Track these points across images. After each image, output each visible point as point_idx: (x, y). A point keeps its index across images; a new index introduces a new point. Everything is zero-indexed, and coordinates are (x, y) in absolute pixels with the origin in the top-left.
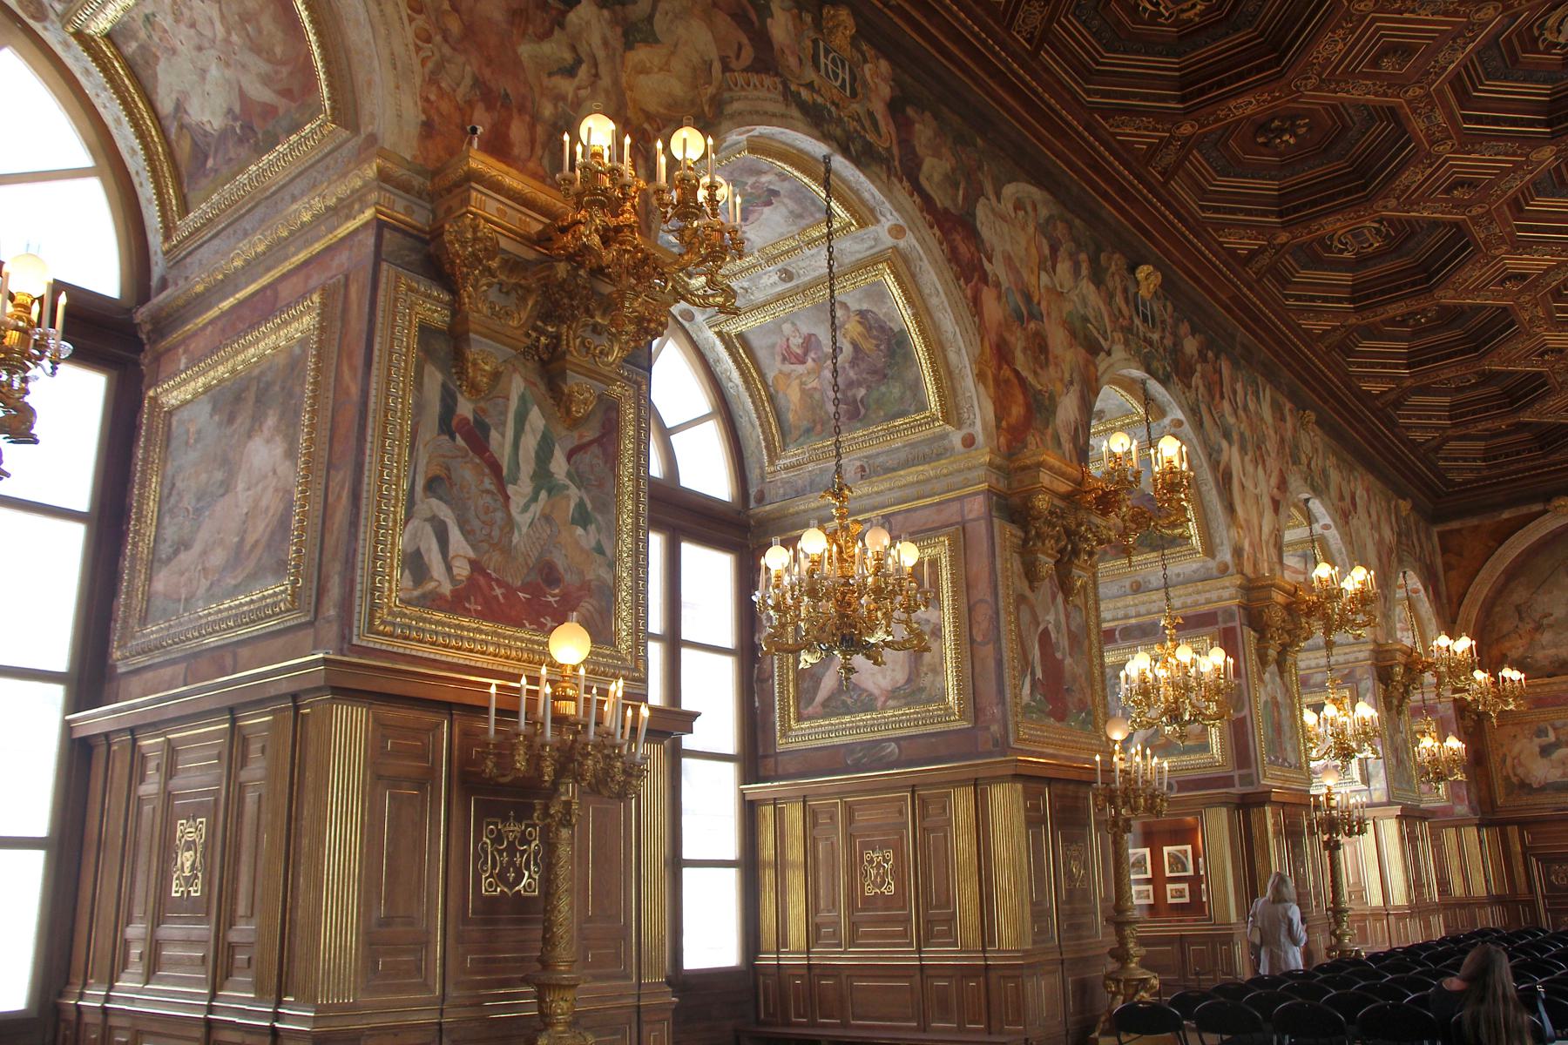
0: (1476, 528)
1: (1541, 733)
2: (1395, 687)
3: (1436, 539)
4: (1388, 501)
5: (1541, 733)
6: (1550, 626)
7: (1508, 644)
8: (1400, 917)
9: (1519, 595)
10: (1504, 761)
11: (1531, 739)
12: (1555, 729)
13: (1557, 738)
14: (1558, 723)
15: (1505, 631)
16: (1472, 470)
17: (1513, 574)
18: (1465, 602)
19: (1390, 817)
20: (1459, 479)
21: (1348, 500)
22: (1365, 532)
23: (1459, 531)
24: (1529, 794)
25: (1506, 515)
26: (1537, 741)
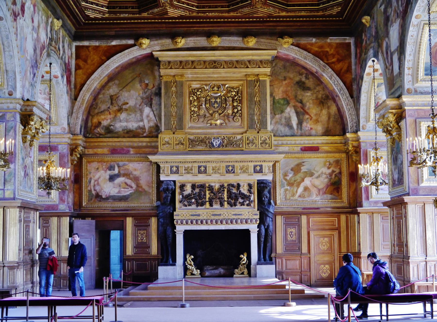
0: (96, 47)
1: (111, 168)
2: (30, 129)
3: (74, 50)
4: (48, 18)
5: (111, 168)
6: (126, 110)
7: (103, 117)
8: (11, 268)
9: (113, 90)
10: (90, 182)
11: (106, 171)
12: (119, 167)
13: (119, 172)
14: (121, 163)
15: (102, 109)
16: (100, 12)
17: (111, 78)
18: (84, 89)
19: (14, 207)
20: (92, 16)
21: (19, 6)
22: (28, 31)
23: (87, 47)
24: (100, 201)
25: (114, 43)
26: (109, 172)
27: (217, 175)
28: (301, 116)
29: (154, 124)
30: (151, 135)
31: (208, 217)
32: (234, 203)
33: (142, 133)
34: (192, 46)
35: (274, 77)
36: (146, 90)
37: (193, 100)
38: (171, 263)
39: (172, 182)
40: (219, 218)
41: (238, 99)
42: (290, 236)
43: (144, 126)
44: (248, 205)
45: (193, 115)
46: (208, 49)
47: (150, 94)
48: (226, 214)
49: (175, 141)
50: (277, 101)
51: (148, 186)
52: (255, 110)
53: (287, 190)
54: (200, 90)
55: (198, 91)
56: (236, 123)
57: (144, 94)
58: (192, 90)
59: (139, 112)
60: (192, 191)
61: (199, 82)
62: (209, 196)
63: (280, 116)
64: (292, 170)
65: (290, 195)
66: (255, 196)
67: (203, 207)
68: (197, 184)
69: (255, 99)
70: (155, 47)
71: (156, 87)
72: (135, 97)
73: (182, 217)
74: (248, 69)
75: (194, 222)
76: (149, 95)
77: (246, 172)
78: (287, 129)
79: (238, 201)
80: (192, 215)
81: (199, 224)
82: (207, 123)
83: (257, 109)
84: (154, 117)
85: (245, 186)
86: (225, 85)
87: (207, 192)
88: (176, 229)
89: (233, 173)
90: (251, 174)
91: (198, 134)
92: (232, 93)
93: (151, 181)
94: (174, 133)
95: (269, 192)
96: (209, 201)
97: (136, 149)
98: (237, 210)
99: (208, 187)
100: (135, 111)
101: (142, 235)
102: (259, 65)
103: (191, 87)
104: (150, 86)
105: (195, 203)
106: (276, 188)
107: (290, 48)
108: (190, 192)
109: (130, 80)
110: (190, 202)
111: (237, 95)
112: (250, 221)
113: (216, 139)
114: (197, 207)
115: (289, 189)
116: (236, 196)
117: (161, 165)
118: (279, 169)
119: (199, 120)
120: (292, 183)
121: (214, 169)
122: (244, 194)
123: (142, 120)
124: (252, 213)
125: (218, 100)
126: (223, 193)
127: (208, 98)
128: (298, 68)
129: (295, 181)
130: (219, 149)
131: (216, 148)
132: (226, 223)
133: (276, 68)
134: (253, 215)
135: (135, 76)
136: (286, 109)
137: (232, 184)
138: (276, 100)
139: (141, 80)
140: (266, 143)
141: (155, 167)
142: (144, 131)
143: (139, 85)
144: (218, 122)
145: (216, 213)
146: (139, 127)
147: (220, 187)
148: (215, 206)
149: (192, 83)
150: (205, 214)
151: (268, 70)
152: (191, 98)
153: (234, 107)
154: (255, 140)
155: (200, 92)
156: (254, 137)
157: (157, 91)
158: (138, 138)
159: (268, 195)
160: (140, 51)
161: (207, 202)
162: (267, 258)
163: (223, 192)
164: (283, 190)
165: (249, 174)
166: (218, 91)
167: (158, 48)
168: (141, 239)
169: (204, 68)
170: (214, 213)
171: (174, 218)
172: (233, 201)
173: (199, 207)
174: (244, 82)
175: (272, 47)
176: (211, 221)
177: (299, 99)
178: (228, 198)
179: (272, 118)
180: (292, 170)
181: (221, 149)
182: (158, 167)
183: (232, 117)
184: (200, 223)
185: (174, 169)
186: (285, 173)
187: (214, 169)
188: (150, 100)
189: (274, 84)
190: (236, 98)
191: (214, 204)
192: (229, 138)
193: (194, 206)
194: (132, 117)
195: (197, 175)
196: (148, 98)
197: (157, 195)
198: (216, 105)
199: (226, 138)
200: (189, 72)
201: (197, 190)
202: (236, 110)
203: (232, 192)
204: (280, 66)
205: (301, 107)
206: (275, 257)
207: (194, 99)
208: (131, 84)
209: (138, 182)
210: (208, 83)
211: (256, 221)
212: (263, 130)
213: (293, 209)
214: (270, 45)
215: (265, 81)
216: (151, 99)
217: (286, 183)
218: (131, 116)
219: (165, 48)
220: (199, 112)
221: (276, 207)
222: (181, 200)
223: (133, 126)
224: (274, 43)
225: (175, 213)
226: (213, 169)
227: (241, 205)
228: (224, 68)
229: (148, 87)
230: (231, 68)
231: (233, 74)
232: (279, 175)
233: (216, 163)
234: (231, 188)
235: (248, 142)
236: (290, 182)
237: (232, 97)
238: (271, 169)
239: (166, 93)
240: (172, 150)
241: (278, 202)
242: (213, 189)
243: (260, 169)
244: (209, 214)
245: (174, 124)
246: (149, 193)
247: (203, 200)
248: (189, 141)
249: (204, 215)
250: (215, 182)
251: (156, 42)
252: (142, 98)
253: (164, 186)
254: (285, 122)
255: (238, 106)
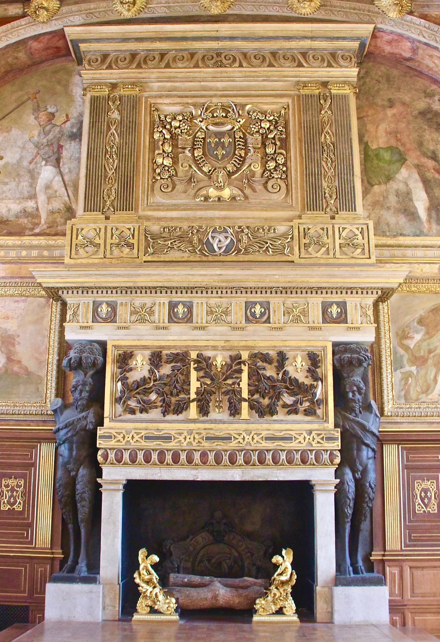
27: (223, 329)
28: (435, 191)
29: (62, 205)
30: (53, 230)
31: (194, 444)
32: (268, 406)
33: (30, 226)
34: (164, 15)
35: (364, 101)
36: (48, 128)
37: (162, 138)
38: (84, 574)
39: (96, 345)
40: (225, 448)
41: (277, 137)
42: (422, 500)
43: (37, 209)
44: (307, 412)
45: (159, 174)
46: (203, 19)
47: (58, 136)
48: (247, 437)
49: (109, 235)
50: (375, 153)
51: (37, 359)
52: (324, 163)
53: (409, 375)
54: (181, 118)
55: (175, 119)
56: (273, 195)
57: (42, 136)
58: (160, 118)
59: (27, 177)
60: (151, 371)
61: (178, 100)
62: (198, 384)
63: (383, 187)
64: (421, 322)
65: (419, 389)
66: (326, 387)
67: (181, 417)
68: (165, 352)
69: (323, 140)
70: (71, 18)
71: (72, 121)
72: (20, 143)
73: (119, 441)
74: (301, 69)
75: (155, 457)
76: (55, 137)
77: (301, 321)
78: (402, 220)
79: (278, 401)
80: (147, 438)
81: (168, 464)
82: (195, 196)
83: (326, 163)
84: (64, 189)
85: (299, 359)
86: (243, 106)
87: (194, 375)
88: (101, 477)
89: (265, 322)
90: (316, 325)
91: (172, 219)
92: (263, 125)
93: (44, 347)
94: (107, 218)
95: (365, 379)
96: (198, 400)
97: (13, 266)
98: (277, 426)
99: (196, 362)
100: (18, 175)
101: (12, 492)
102: (329, 62)
103: (157, 110)
104: (59, 119)
105: (159, 404)
106: (381, 368)
107: (405, 21)
108: (147, 375)
109: (14, 106)
110: (144, 402)
111: (275, 128)
112: (313, 457)
113: (220, 233)
114: (164, 416)
115: (415, 372)
116: (273, 387)
117: (69, 302)
118: (386, 320)
119: (177, 187)
120: (423, 357)
121: (212, 312)
122: (296, 380)
123: (33, 197)
124: (319, 435)
125: (226, 140)
126: (236, 378)
127: (200, 135)
128: (421, 83)
129: (430, 352)
130: (228, 258)
131: (220, 254)
132: (247, 462)
133: (368, 80)
134: (322, 439)
135: (26, 97)
136: (398, 171)
137: (261, 353)
138: (373, 150)
139: (38, 106)
140: (355, 246)
141: (57, 307)
142: (36, 221)
143: (32, 117)
144: (226, 193)
145: (218, 434)
146: (25, 213)
147: (228, 360)
148: (214, 414)
149: (159, 101)
150: (185, 433)
151: (353, 72)
152: (156, 136)
153: (265, 159)
154: (325, 238)
155: (180, 121)
156: (323, 229)
157: (75, 130)
158: (18, 238)
159: (362, 385)
160: (34, 27)
161: (193, 400)
162: (360, 563)
163: (236, 375)
164: (398, 374)
165: (311, 325)
166: (226, 119)
167: (78, 19)
168: (9, 502)
169: (190, 68)
170: (212, 432)
171: (98, 446)
172: (266, 401)
173: (170, 417)
174: (293, 100)
175: (361, 17)
176: (204, 455)
177: (429, 150)
178: (251, 393)
179: (365, 193)
180: (421, 322)
181: (232, 257)
182: (64, 304)
183: (263, 180)
184: (170, 461)
185: (104, 310)
186: (403, 331)
187: (212, 312)
188: (55, 150)
189: (365, 114)
190: (271, 136)
191: (211, 409)
192: (254, 231)
193: (155, 414)
194: (10, 190)
195: (164, 328)
196: (52, 144)
197: (57, 384)
198: (220, 152)
199: (246, 231)
200: (153, 76)
201: (166, 370)
202: (272, 165)
203: (264, 376)
204: (377, 77)
205: (434, 169)
206: (383, 561)
207: (165, 138)
208: (13, 115)
209: (12, 348)
210: (202, 100)
211: (332, 456)
212: (344, 212)
213: (426, 425)
214: (356, 13)
215: (345, 97)
216: (60, 147)
217: (406, 357)
218: (8, 187)
219: (95, 20)
220: (175, 169)
221: (383, 419)
222: (119, 394)
223: (9, 210)
224: (367, 8)
225: (100, 432)
226: (210, 312)
227: (289, 413)
228: (241, 66)
229: (53, 122)
230: (260, 66)
231: (264, 80)
232: (388, 336)
233: (220, 295)
234: (260, 364)
235: (308, 241)
236: (417, 355)
237: (262, 134)
238: (370, 313)
239: (92, 124)
240: (101, 261)
241: (388, 408)
242: (209, 366)
243: (340, 314)
244: (197, 436)
245: (109, 197)
246: (40, 377)
247: (182, 396)
248: (146, 237)
249: (181, 438)
250: (215, 348)
251: (74, 8)
252: (37, 146)
253: (72, 354)
254: (398, 202)
255: (279, 154)
